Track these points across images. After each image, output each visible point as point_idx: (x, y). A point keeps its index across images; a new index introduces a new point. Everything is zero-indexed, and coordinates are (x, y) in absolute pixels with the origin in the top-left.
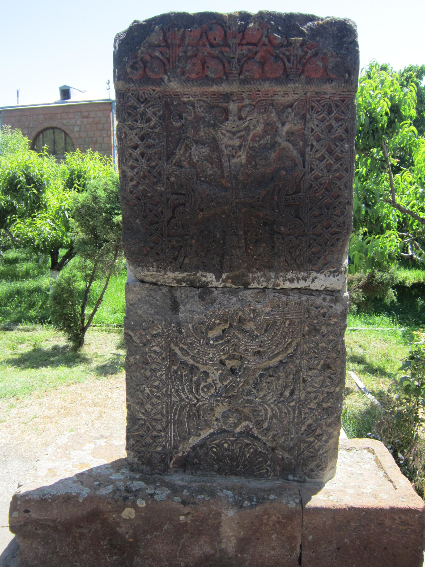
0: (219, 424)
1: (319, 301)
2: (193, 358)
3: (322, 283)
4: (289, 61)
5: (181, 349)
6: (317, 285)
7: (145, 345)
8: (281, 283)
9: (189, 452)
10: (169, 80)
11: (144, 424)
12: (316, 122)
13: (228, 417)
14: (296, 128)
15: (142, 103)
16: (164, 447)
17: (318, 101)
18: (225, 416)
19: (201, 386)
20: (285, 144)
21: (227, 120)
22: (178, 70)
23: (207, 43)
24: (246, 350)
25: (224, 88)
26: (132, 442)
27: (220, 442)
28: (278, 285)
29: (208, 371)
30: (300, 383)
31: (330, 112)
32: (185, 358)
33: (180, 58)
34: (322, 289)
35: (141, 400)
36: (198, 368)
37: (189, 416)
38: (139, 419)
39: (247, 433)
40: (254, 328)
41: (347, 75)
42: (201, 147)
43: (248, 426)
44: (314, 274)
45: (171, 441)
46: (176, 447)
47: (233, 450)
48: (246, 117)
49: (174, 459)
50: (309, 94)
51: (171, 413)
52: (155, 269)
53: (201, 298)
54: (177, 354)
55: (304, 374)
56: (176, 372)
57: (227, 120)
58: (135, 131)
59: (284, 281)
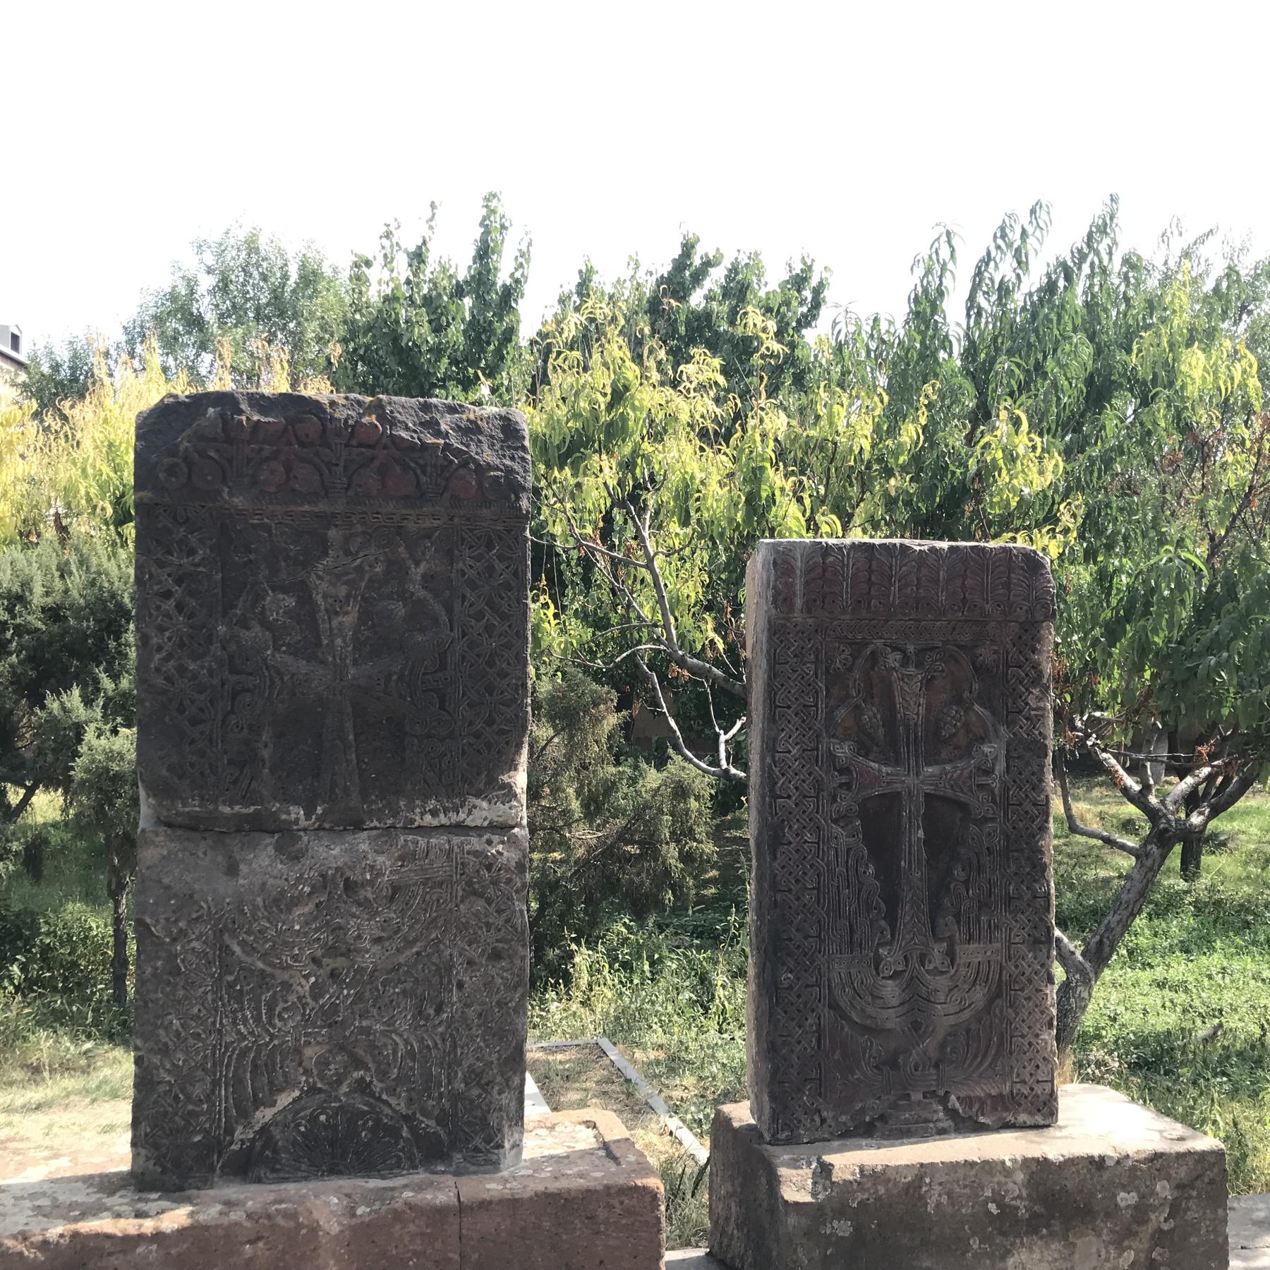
0: (311, 1080)
1: (475, 843)
2: (264, 957)
3: (484, 814)
4: (424, 472)
5: (243, 944)
6: (476, 819)
7: (174, 940)
8: (418, 818)
9: (253, 1140)
10: (231, 494)
11: (170, 1091)
12: (469, 561)
13: (328, 1064)
14: (439, 569)
15: (181, 524)
16: (207, 1132)
17: (471, 531)
18: (323, 1063)
19: (278, 1009)
20: (422, 593)
21: (327, 554)
22: (246, 480)
23: (293, 440)
24: (359, 937)
25: (322, 507)
26: (145, 1128)
27: (312, 1113)
28: (412, 821)
29: (291, 981)
30: (451, 990)
31: (490, 547)
32: (249, 960)
33: (249, 460)
34: (486, 824)
35: (166, 1044)
36: (272, 976)
37: (255, 1067)
38: (159, 1083)
39: (363, 1087)
40: (370, 896)
41: (513, 496)
42: (281, 596)
43: (362, 1078)
44: (472, 800)
45: (220, 1119)
46: (230, 1131)
47: (336, 1126)
48: (357, 552)
49: (225, 1157)
50: (456, 520)
51: (221, 1065)
52: (197, 803)
53: (279, 848)
54: (233, 953)
55: (460, 972)
56: (231, 985)
57: (327, 554)
58: (168, 570)
59: (422, 814)
